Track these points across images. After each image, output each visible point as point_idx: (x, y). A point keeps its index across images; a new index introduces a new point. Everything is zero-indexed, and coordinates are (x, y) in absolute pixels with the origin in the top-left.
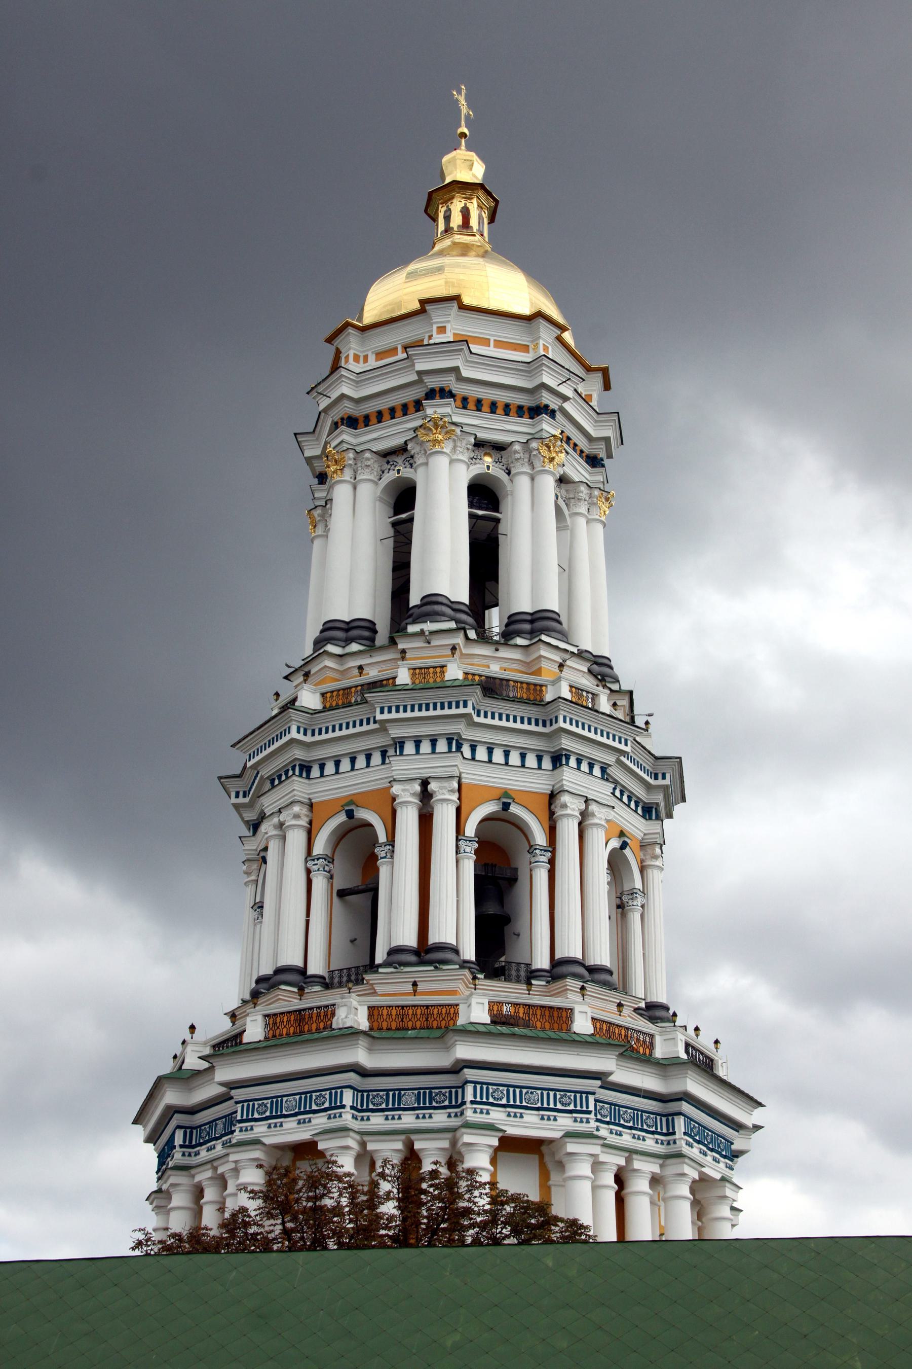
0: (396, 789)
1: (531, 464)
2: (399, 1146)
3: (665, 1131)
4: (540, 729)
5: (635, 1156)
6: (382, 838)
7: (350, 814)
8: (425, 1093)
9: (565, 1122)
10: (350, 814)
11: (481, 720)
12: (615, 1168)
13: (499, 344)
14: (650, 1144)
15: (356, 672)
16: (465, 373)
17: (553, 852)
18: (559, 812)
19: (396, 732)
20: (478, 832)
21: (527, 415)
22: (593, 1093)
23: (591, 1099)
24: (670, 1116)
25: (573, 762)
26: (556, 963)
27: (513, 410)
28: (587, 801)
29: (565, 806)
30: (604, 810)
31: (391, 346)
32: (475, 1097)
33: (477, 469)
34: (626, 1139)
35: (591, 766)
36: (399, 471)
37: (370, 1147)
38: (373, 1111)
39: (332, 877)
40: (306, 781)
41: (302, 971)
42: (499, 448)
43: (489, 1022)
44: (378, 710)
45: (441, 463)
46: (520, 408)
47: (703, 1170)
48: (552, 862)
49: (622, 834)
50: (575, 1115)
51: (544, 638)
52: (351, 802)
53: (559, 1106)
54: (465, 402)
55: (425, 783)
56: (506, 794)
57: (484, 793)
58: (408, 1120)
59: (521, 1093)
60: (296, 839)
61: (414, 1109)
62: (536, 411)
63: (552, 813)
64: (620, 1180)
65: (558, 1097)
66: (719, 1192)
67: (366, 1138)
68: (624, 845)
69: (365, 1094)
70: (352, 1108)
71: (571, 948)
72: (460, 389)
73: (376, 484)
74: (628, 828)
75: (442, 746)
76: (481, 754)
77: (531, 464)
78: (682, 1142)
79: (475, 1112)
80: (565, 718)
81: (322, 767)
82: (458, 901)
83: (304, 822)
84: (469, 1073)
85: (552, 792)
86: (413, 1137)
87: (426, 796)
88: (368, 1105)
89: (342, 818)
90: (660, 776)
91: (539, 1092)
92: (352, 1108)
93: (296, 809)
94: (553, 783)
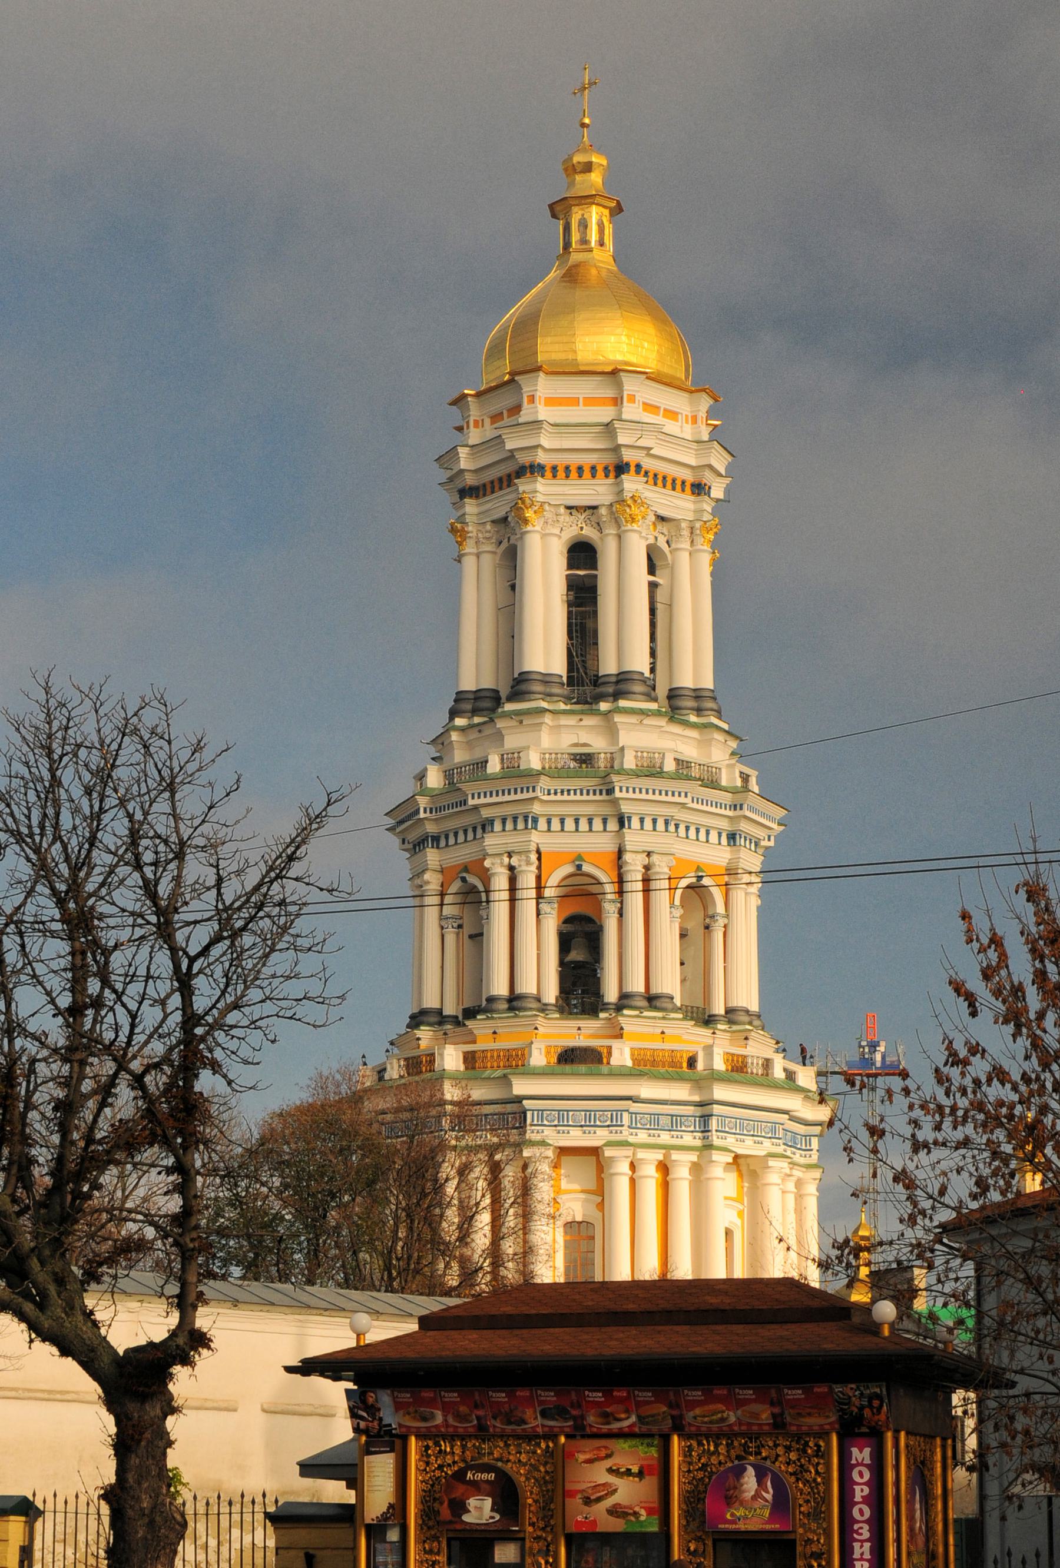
4: (604, 797)
10: (464, 880)
17: (622, 903)
19: (486, 813)
21: (612, 474)
23: (625, 1115)
30: (666, 858)
34: (665, 1138)
41: (439, 1012)
42: (595, 508)
48: (621, 913)
49: (698, 869)
52: (466, 869)
53: (598, 1123)
56: (580, 857)
64: (664, 1168)
68: (700, 878)
73: (494, 553)
77: (619, 527)
80: (621, 788)
82: (538, 955)
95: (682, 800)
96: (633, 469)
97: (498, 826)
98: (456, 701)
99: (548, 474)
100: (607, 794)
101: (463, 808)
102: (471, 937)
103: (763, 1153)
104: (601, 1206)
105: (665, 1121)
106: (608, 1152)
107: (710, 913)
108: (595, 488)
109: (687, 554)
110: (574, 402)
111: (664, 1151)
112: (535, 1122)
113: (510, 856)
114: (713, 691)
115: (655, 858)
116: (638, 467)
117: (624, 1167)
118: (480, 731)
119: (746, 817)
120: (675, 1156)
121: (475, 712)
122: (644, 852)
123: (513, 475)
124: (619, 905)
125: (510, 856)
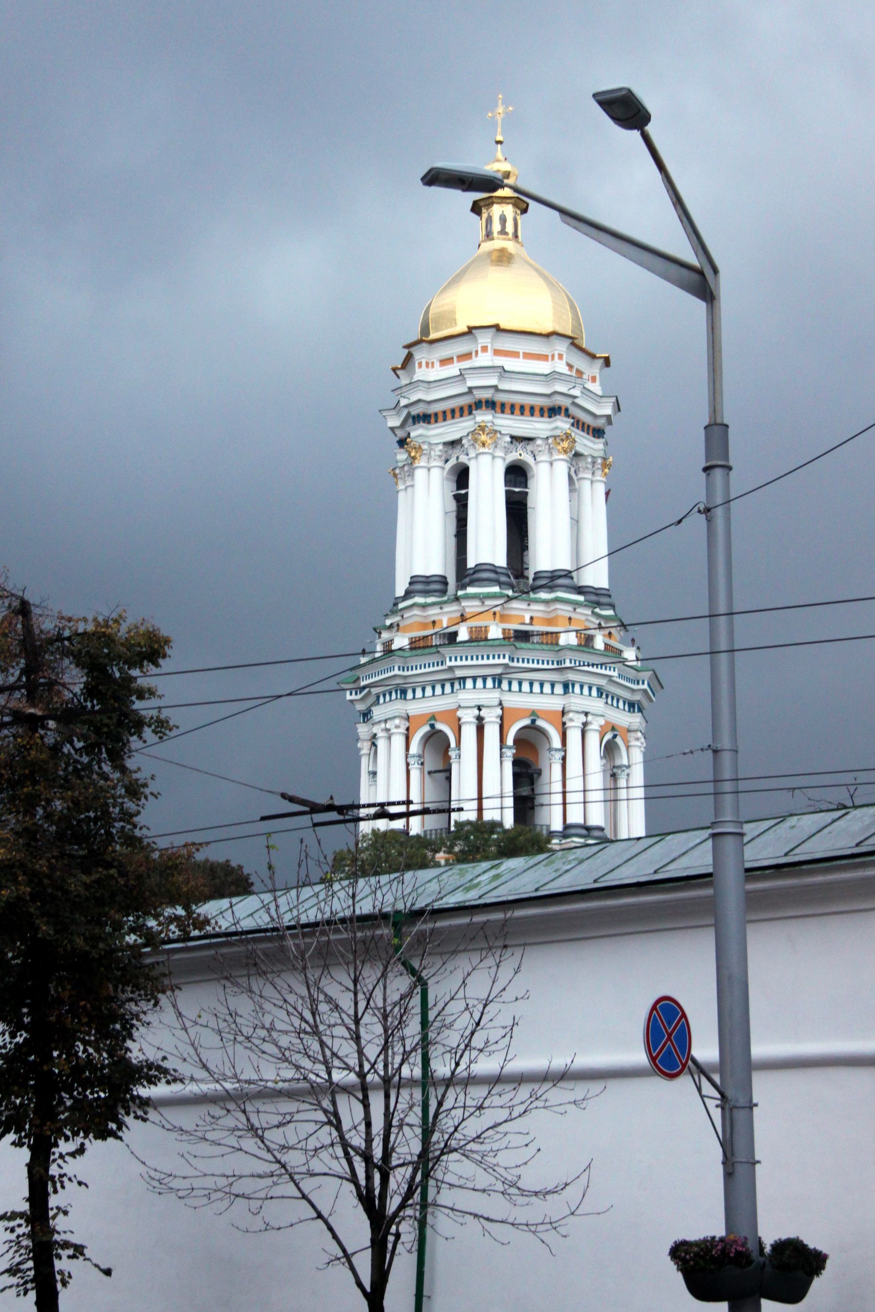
0: (459, 713)
7: (432, 726)
10: (432, 726)
11: (515, 664)
13: (528, 356)
15: (431, 625)
17: (565, 751)
18: (568, 724)
19: (459, 673)
20: (516, 741)
21: (546, 414)
26: (567, 827)
27: (537, 412)
29: (571, 720)
31: (449, 356)
35: (590, 689)
36: (458, 458)
40: (404, 701)
42: (530, 440)
44: (448, 659)
45: (485, 460)
46: (542, 410)
48: (564, 759)
49: (613, 729)
51: (561, 594)
57: (519, 713)
60: (398, 741)
62: (553, 411)
63: (564, 724)
68: (615, 736)
71: (575, 816)
72: (500, 398)
73: (443, 468)
83: (402, 730)
85: (564, 708)
87: (480, 719)
89: (427, 728)
90: (641, 682)
93: (397, 721)
94: (564, 703)
95: (611, 673)
96: (563, 411)
97: (469, 683)
98: (410, 584)
99: (498, 408)
100: (558, 664)
101: (440, 668)
102: (430, 773)
107: (617, 763)
108: (534, 424)
109: (589, 482)
110: (514, 354)
113: (479, 709)
114: (608, 590)
115: (590, 718)
116: (567, 410)
118: (441, 608)
121: (426, 593)
122: (583, 712)
123: (474, 407)
124: (563, 753)
125: (479, 709)
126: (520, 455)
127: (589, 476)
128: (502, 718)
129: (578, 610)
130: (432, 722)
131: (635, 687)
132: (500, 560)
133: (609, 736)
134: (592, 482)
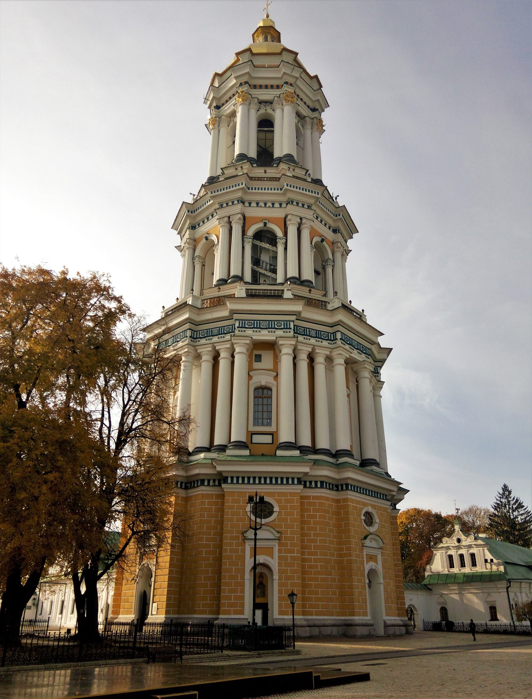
1: (282, 105)
2: (210, 349)
3: (332, 339)
4: (279, 191)
5: (316, 347)
6: (216, 242)
7: (207, 238)
8: (222, 329)
9: (280, 333)
10: (207, 238)
12: (308, 353)
14: (325, 343)
16: (254, 75)
18: (288, 223)
22: (293, 321)
24: (334, 333)
25: (295, 203)
26: (286, 280)
28: (301, 219)
32: (239, 325)
33: (262, 111)
37: (199, 351)
38: (201, 338)
39: (204, 265)
43: (245, 296)
47: (352, 355)
50: (283, 330)
53: (276, 327)
54: (255, 87)
55: (229, 218)
58: (215, 339)
59: (260, 323)
61: (217, 335)
64: (311, 359)
65: (276, 323)
66: (363, 366)
67: (197, 348)
68: (322, 241)
69: (198, 332)
70: (191, 337)
72: (253, 82)
74: (325, 235)
75: (236, 202)
76: (254, 204)
78: (339, 342)
79: (239, 331)
81: (199, 225)
84: (236, 316)
86: (215, 345)
88: (199, 336)
91: (268, 322)
92: (191, 337)
95: (316, 195)
103: (361, 360)
104: (276, 377)
105: (313, 333)
106: (280, 342)
111: (312, 347)
112: (241, 326)
117: (290, 351)
119: (342, 218)
120: (317, 351)
124: (285, 240)
126: (266, 110)
127: (310, 128)
128: (244, 224)
129: (295, 171)
130: (207, 235)
131: (335, 218)
132: (253, 153)
133: (316, 239)
134: (311, 133)
